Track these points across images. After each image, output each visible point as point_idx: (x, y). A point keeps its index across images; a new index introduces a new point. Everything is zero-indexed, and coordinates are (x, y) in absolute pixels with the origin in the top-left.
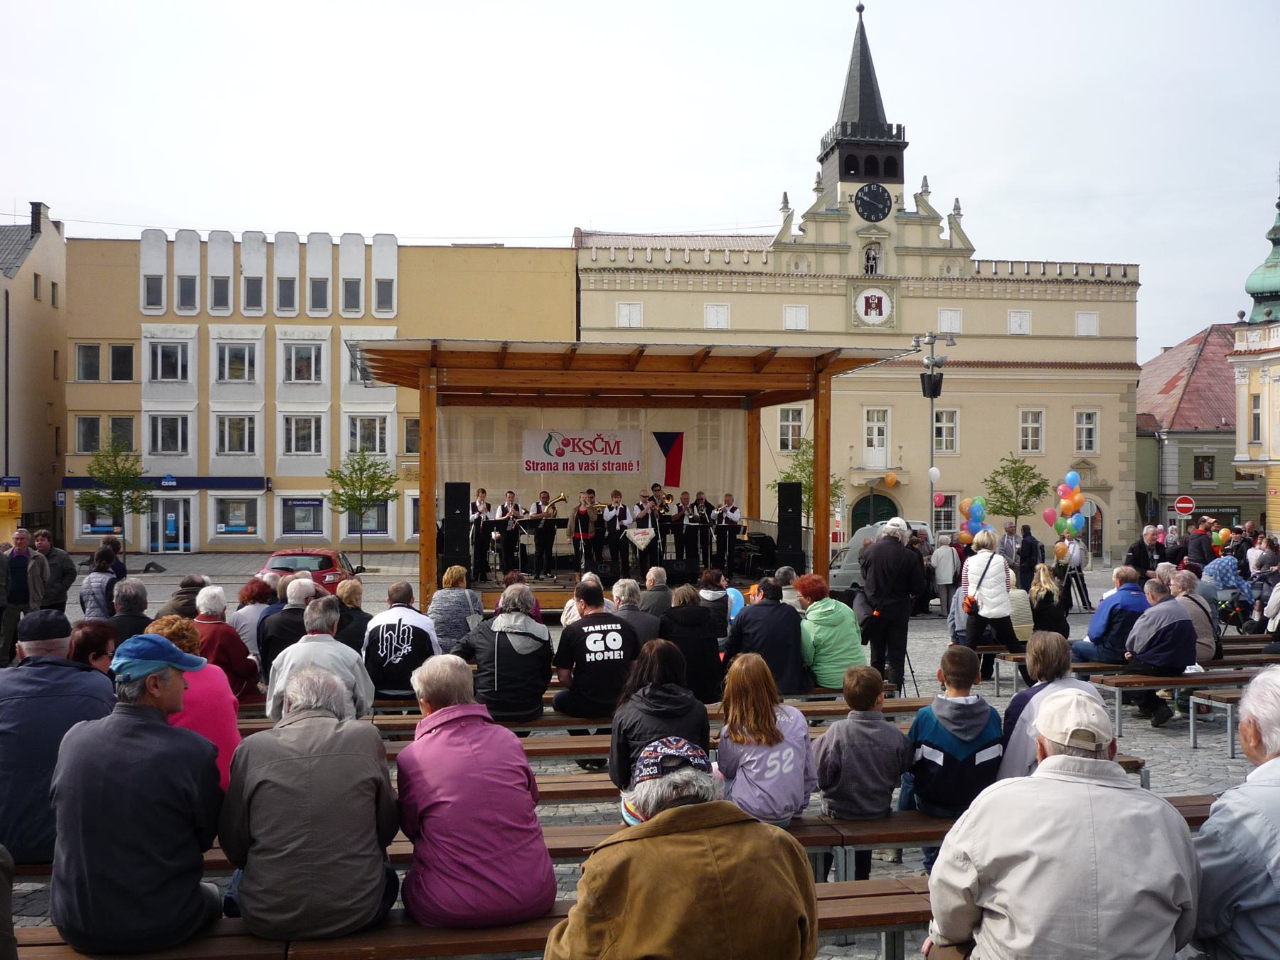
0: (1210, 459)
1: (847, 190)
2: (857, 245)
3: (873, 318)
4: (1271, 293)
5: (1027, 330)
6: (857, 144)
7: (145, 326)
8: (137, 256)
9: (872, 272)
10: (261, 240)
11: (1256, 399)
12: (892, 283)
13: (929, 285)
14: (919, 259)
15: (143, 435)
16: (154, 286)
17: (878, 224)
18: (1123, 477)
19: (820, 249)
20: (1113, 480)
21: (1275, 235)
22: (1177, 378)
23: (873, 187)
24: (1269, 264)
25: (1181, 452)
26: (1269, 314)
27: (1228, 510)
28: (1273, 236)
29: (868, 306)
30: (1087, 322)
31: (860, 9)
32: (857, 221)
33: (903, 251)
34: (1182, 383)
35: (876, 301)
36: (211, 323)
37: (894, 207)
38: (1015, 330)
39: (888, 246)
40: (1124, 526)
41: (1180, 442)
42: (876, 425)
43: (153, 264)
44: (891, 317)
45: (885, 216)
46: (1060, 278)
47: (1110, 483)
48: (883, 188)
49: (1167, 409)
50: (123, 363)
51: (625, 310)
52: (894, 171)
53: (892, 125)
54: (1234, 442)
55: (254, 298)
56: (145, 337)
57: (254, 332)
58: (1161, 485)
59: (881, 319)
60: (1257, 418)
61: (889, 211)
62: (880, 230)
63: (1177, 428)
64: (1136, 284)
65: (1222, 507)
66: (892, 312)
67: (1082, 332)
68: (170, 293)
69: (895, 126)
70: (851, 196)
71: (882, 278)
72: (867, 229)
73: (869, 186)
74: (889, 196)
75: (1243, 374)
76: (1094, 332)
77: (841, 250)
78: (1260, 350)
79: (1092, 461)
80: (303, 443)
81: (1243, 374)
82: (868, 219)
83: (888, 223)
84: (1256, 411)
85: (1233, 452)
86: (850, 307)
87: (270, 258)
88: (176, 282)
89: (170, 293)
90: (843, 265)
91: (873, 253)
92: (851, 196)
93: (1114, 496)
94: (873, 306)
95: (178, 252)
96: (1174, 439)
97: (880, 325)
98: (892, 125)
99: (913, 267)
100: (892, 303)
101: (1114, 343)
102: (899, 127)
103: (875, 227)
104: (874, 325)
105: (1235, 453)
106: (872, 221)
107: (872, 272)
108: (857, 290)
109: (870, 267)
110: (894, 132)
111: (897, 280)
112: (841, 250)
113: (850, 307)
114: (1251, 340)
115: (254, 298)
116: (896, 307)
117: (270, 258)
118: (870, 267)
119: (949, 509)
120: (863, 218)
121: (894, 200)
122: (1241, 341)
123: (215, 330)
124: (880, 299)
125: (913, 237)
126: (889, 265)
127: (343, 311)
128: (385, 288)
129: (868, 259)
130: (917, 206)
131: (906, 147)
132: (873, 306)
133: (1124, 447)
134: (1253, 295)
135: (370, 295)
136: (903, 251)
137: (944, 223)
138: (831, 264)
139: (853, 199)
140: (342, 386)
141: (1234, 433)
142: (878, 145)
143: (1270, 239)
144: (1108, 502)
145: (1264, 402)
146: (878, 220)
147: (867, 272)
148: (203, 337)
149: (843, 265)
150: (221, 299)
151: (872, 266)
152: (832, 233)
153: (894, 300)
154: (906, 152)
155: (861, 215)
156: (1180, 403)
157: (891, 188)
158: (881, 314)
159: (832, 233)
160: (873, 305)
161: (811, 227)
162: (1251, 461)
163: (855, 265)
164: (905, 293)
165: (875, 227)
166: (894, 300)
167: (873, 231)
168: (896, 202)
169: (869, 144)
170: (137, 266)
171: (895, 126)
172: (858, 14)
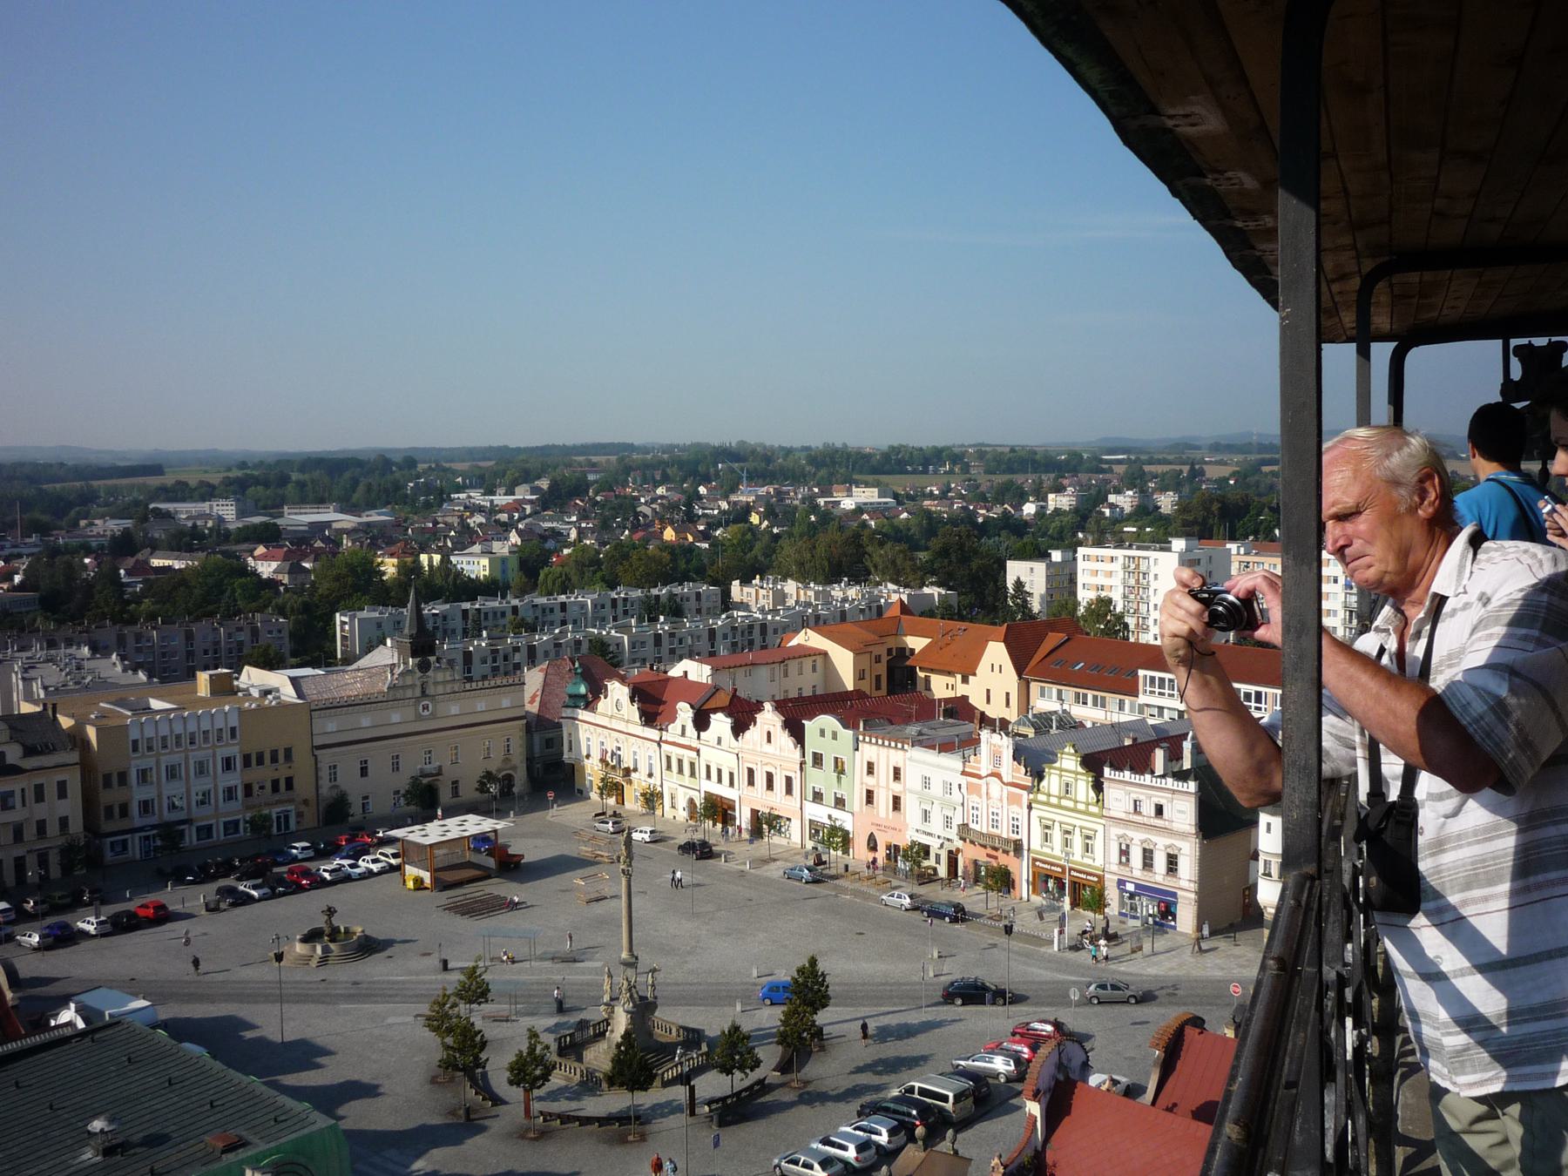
0: (552, 739)
2: (418, 683)
3: (426, 713)
7: (133, 762)
12: (432, 697)
15: (135, 809)
16: (135, 742)
29: (424, 709)
30: (506, 703)
32: (419, 674)
33: (436, 683)
34: (538, 699)
39: (431, 681)
43: (134, 734)
50: (123, 778)
51: (330, 725)
60: (570, 741)
62: (428, 677)
64: (524, 684)
68: (142, 746)
71: (428, 696)
72: (421, 677)
76: (509, 705)
77: (413, 686)
83: (430, 673)
85: (562, 754)
86: (417, 710)
87: (185, 723)
95: (146, 727)
99: (440, 689)
108: (420, 703)
109: (424, 694)
111: (434, 696)
113: (417, 710)
115: (178, 744)
117: (185, 723)
118: (423, 692)
123: (163, 758)
126: (431, 690)
128: (233, 730)
135: (226, 735)
136: (436, 683)
138: (409, 693)
152: (409, 680)
159: (409, 680)
160: (426, 708)
161: (401, 679)
163: (418, 692)
170: (128, 737)
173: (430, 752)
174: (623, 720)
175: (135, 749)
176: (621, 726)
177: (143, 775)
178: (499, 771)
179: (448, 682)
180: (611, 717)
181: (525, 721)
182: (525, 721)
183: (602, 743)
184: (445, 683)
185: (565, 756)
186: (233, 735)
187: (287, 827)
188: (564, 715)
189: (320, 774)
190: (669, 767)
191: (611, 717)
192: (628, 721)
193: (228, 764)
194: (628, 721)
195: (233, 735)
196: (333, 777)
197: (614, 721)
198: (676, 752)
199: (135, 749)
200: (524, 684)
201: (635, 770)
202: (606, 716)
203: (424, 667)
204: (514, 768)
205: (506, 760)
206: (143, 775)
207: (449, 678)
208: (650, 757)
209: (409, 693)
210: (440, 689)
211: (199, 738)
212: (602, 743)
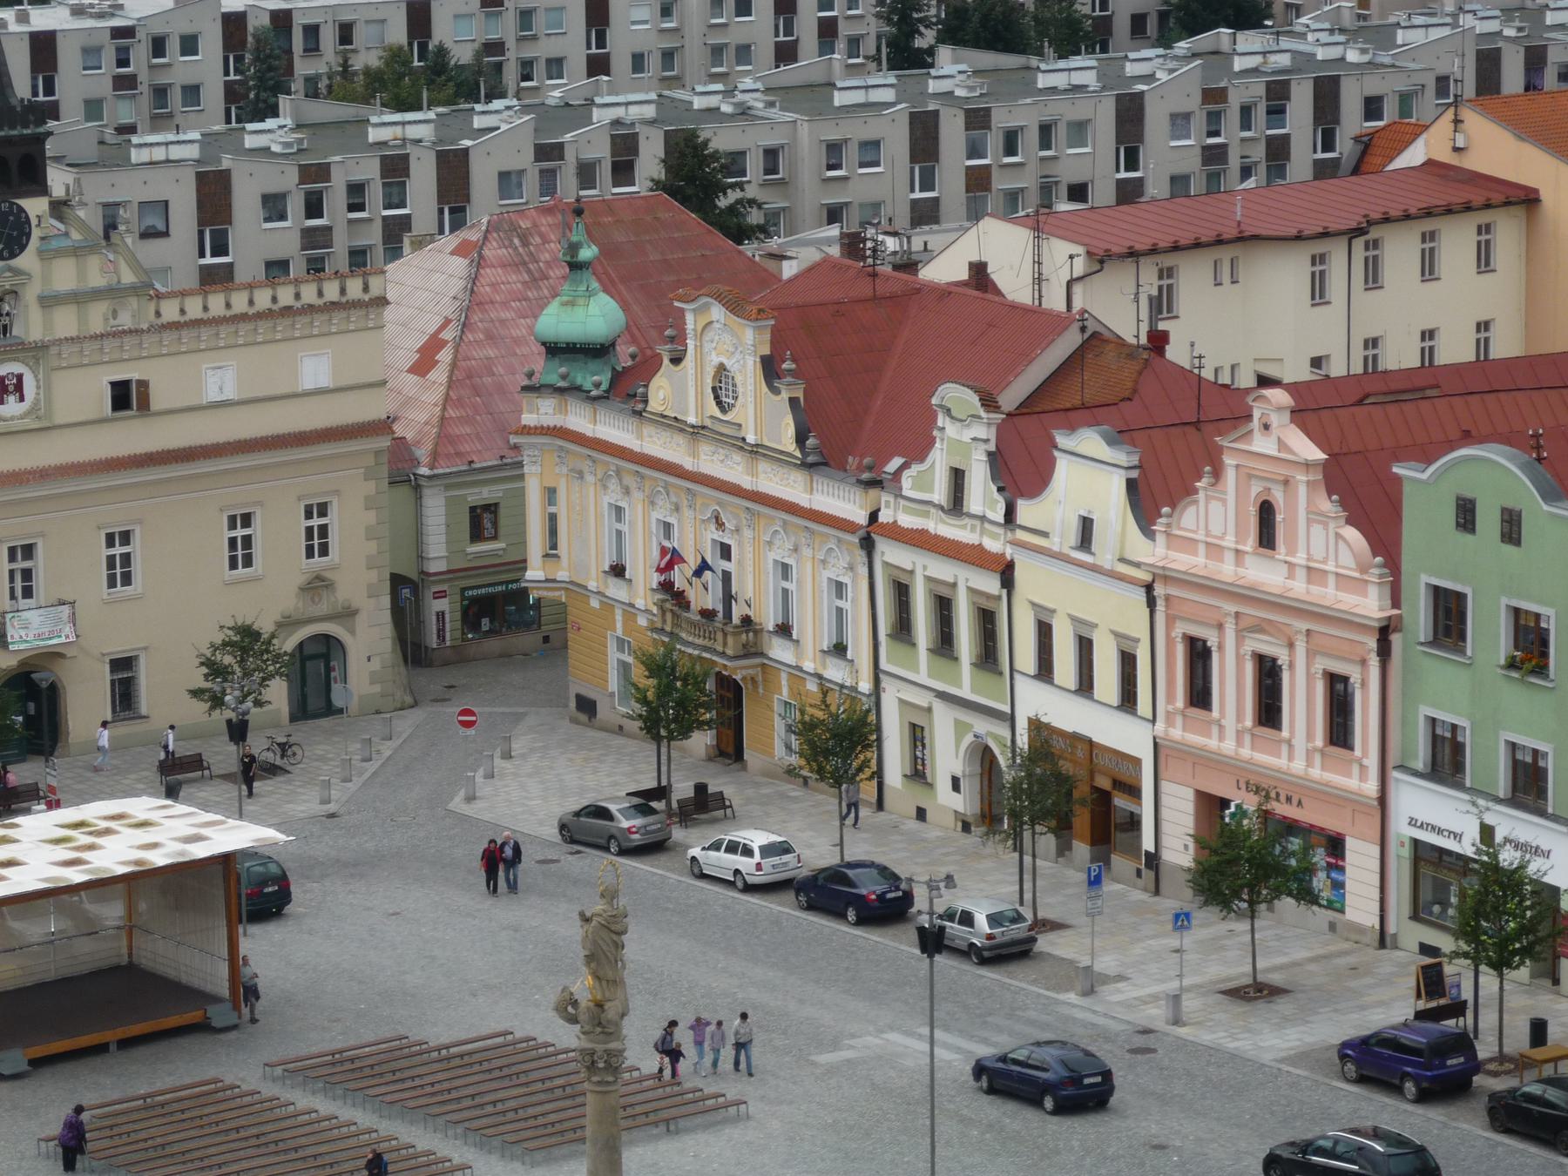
4: (568, 344)
5: (230, 394)
11: (551, 494)
13: (88, 347)
20: (359, 599)
30: (315, 369)
33: (49, 301)
35: (15, 381)
38: (213, 395)
39: (31, 294)
40: (376, 665)
44: (37, 402)
45: (23, 248)
46: (275, 307)
47: (355, 605)
59: (25, 406)
60: (553, 518)
62: (17, 272)
64: (382, 301)
66: (38, 394)
67: (308, 384)
74: (27, 217)
75: (534, 459)
76: (325, 381)
79: (327, 575)
81: (534, 459)
84: (552, 509)
85: (522, 564)
93: (361, 621)
94: (11, 388)
97: (22, 417)
99: (65, 322)
100: (38, 381)
101: (352, 395)
103: (10, 269)
104: (12, 418)
105: (525, 569)
114: (542, 411)
116: (46, 387)
119: (130, 675)
121: (34, 222)
122: (531, 412)
124: (20, 377)
132: (11, 388)
133: (372, 547)
134: (544, 344)
136: (49, 301)
144: (352, 632)
145: (562, 495)
146: (13, 255)
153: (41, 376)
158: (22, 399)
162: (547, 581)
164: (55, 363)
166: (41, 376)
167: (8, 274)
168: (39, 225)
173: (28, 551)
174: (740, 444)
176: (732, 469)
178: (287, 624)
179: (97, 294)
180: (697, 432)
181: (384, 442)
182: (384, 442)
183: (667, 527)
184: (79, 298)
185: (534, 573)
188: (528, 419)
191: (697, 432)
192: (756, 452)
194: (756, 452)
197: (705, 448)
198: (926, 569)
200: (382, 301)
201: (784, 630)
202: (675, 424)
204: (347, 615)
205: (317, 585)
207: (97, 280)
210: (65, 322)
212: (667, 527)
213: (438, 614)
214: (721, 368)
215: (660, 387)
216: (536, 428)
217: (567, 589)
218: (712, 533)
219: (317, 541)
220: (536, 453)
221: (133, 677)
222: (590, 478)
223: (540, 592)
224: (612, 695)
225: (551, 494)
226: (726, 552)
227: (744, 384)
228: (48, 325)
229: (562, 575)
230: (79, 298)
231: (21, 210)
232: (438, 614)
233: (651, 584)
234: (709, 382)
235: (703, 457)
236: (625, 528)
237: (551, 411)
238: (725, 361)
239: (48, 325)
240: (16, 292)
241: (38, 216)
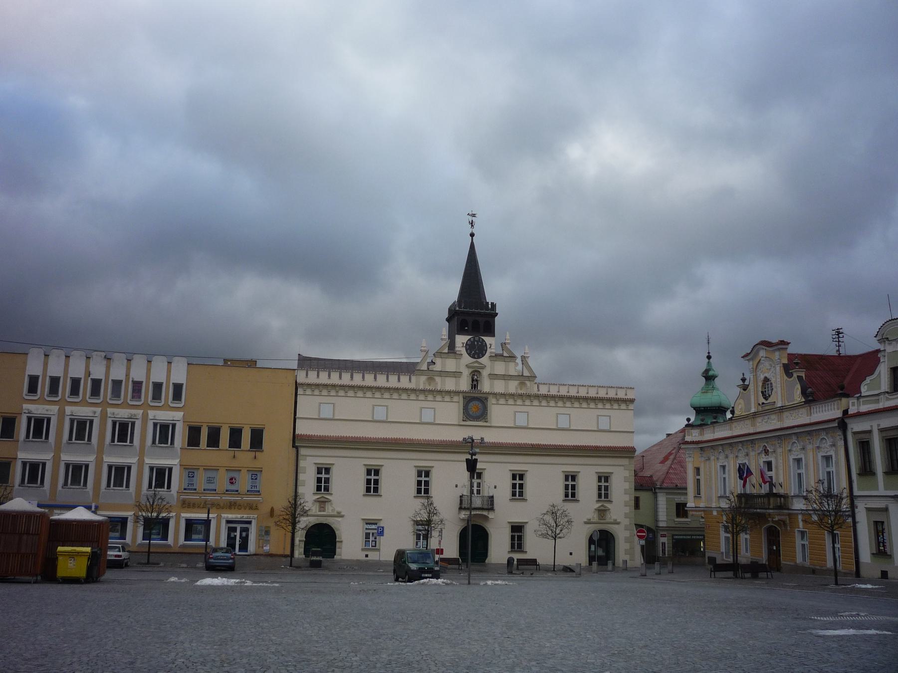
1: (461, 340)
2: (466, 373)
4: (704, 407)
6: (468, 313)
7: (25, 406)
8: (25, 363)
9: (475, 389)
10: (103, 356)
11: (698, 470)
14: (503, 381)
16: (33, 382)
17: (479, 360)
18: (626, 516)
19: (443, 374)
21: (706, 374)
22: (670, 454)
23: (477, 338)
24: (704, 391)
25: (668, 500)
26: (702, 420)
27: (698, 537)
28: (705, 375)
31: (472, 235)
32: (467, 359)
33: (493, 377)
36: (67, 406)
37: (489, 350)
39: (485, 373)
41: (667, 494)
42: (475, 481)
43: (34, 367)
48: (482, 339)
49: (661, 474)
52: (489, 330)
53: (488, 303)
54: (686, 494)
55: (96, 390)
56: (25, 413)
57: (95, 413)
58: (657, 521)
60: (698, 481)
61: (486, 353)
63: (665, 485)
65: (693, 535)
68: (44, 387)
69: (490, 303)
70: (463, 343)
73: (474, 338)
74: (486, 344)
77: (457, 374)
78: (699, 441)
80: (118, 483)
82: (473, 357)
83: (484, 360)
84: (698, 477)
88: (48, 380)
89: (44, 387)
90: (457, 384)
91: (476, 377)
92: (463, 343)
96: (664, 492)
98: (488, 303)
101: (618, 434)
102: (492, 304)
106: (475, 358)
107: (475, 389)
110: (490, 306)
112: (457, 374)
114: (694, 435)
115: (96, 390)
119: (520, 534)
120: (470, 356)
125: (500, 368)
127: (151, 402)
128: (178, 388)
129: (473, 380)
130: (503, 350)
131: (496, 315)
134: (695, 408)
135: (167, 393)
136: (493, 377)
137: (519, 361)
139: (465, 345)
140: (146, 448)
141: (686, 489)
142: (479, 314)
143: (704, 377)
146: (479, 358)
147: (472, 388)
148: (61, 414)
149: (457, 384)
150: (75, 391)
151: (475, 385)
152: (450, 365)
154: (496, 318)
155: (469, 354)
156: (669, 470)
157: (488, 340)
162: (696, 507)
163: (464, 384)
165: (477, 362)
169: (474, 313)
170: (24, 369)
171: (490, 303)
172: (471, 238)
175: (33, 389)
177: (39, 427)
184: (506, 377)
186: (177, 395)
187: (244, 546)
189: (301, 477)
190: (867, 470)
193: (164, 432)
195: (177, 395)
196: (323, 485)
199: (33, 389)
203: (477, 350)
206: (39, 427)
208: (828, 458)
209: (450, 384)
210: (499, 387)
211: (127, 390)
213: (662, 543)
214: (766, 380)
215: (740, 403)
216: (691, 442)
217: (704, 511)
218: (764, 458)
219: (603, 493)
220: (691, 453)
221: (521, 536)
222: (712, 458)
223: (693, 512)
224: (722, 553)
225: (698, 470)
226: (769, 464)
227: (776, 382)
228: (492, 386)
229: (702, 505)
230: (506, 377)
231: (482, 339)
232: (662, 543)
233: (738, 492)
234: (760, 389)
235: (758, 424)
236: (726, 476)
237: (697, 435)
238: (767, 375)
239: (492, 386)
240: (480, 372)
241: (490, 344)
